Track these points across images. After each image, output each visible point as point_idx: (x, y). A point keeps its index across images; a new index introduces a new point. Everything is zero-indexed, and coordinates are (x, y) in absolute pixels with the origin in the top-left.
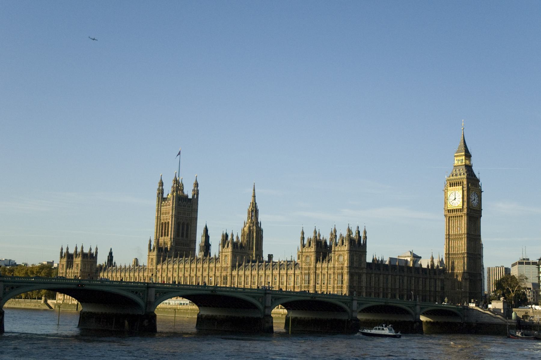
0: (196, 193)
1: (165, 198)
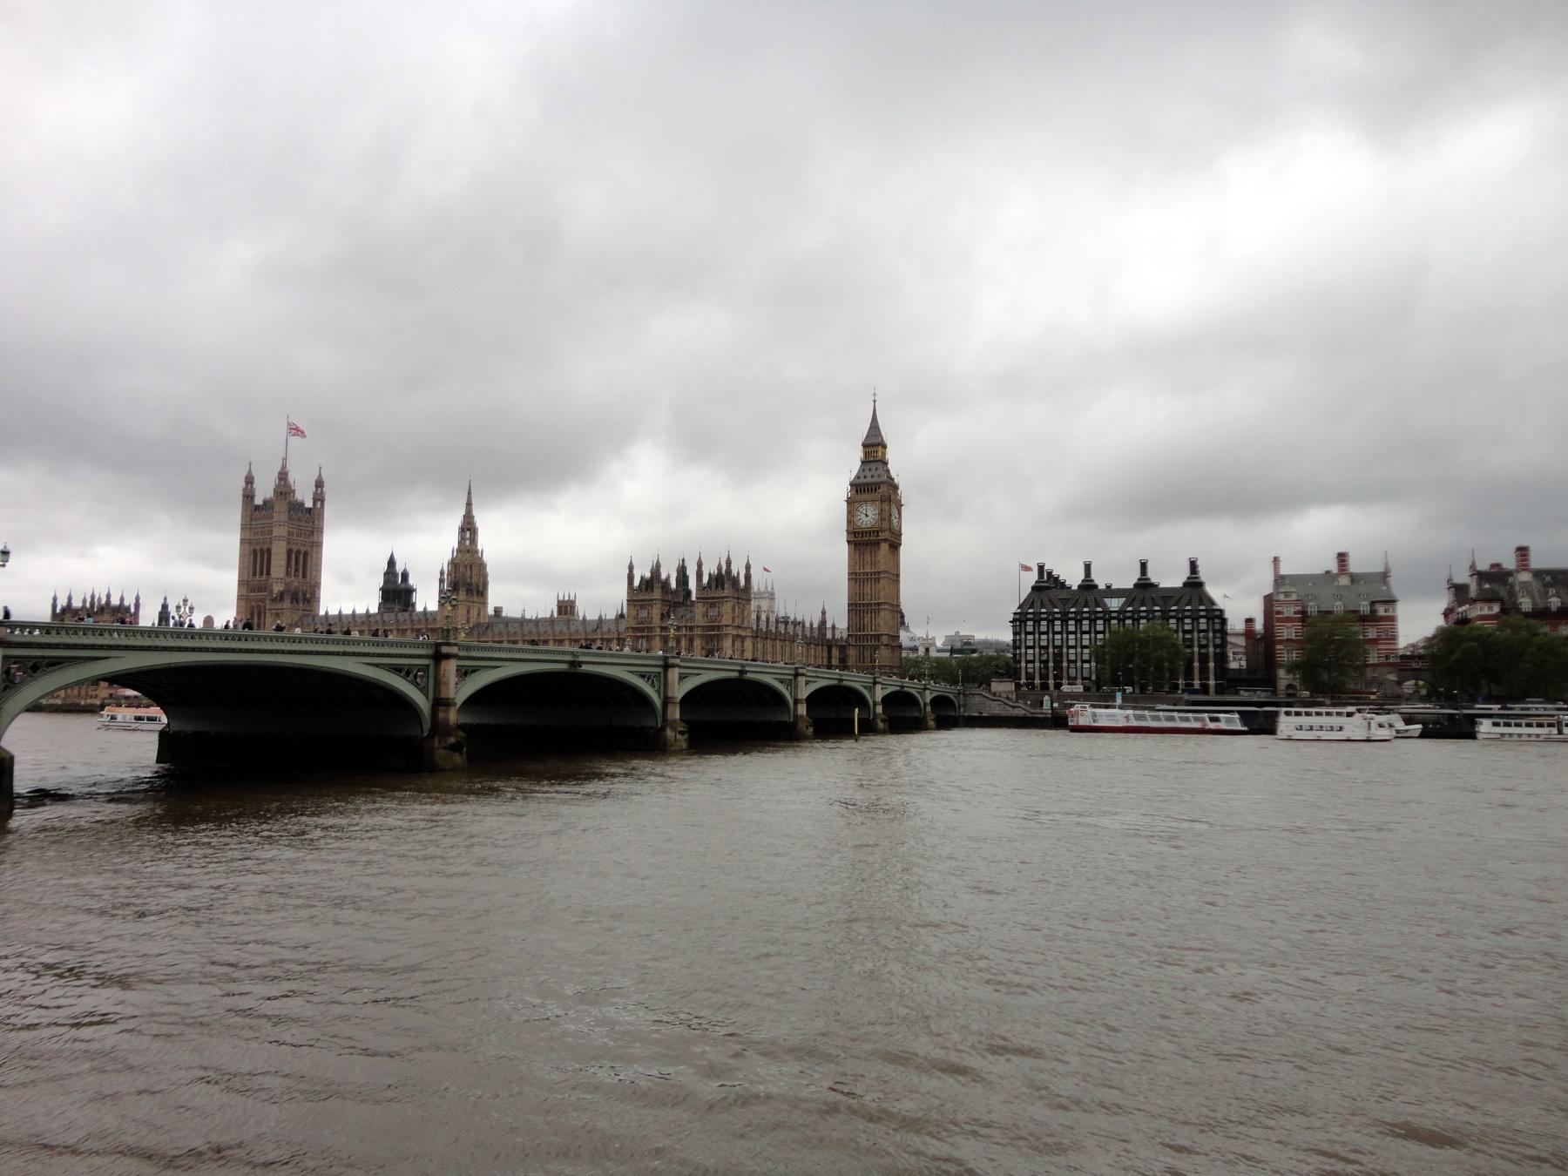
0: (319, 498)
1: (256, 506)
